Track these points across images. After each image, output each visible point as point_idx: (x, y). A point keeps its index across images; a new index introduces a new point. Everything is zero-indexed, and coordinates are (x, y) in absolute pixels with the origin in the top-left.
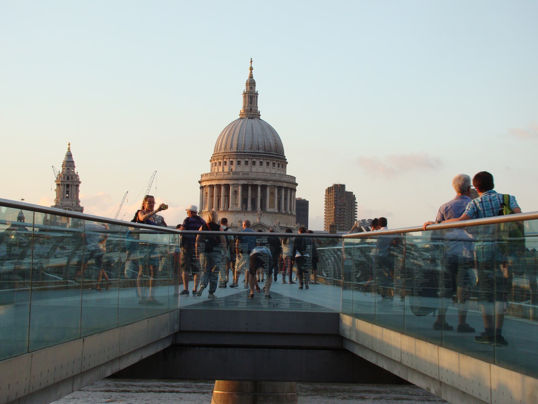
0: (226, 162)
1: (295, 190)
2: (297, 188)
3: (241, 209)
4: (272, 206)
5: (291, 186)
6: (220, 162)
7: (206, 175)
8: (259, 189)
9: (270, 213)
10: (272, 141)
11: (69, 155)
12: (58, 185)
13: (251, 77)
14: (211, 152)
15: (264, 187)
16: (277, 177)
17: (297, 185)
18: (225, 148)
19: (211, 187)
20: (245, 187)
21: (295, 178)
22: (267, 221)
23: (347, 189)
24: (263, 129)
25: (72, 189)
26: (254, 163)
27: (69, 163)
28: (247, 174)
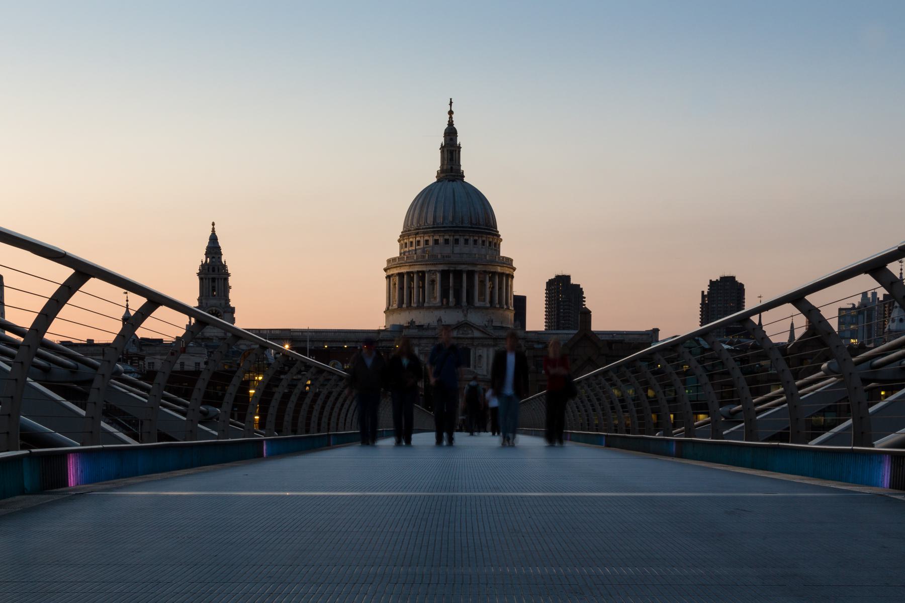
0: (419, 242)
1: (513, 277)
2: (515, 274)
3: (440, 304)
5: (507, 271)
6: (412, 242)
7: (394, 259)
8: (465, 277)
9: (479, 308)
11: (214, 239)
12: (201, 279)
14: (399, 229)
17: (514, 269)
18: (418, 222)
19: (401, 275)
20: (445, 274)
21: (512, 260)
22: (475, 318)
26: (457, 241)
27: (214, 249)
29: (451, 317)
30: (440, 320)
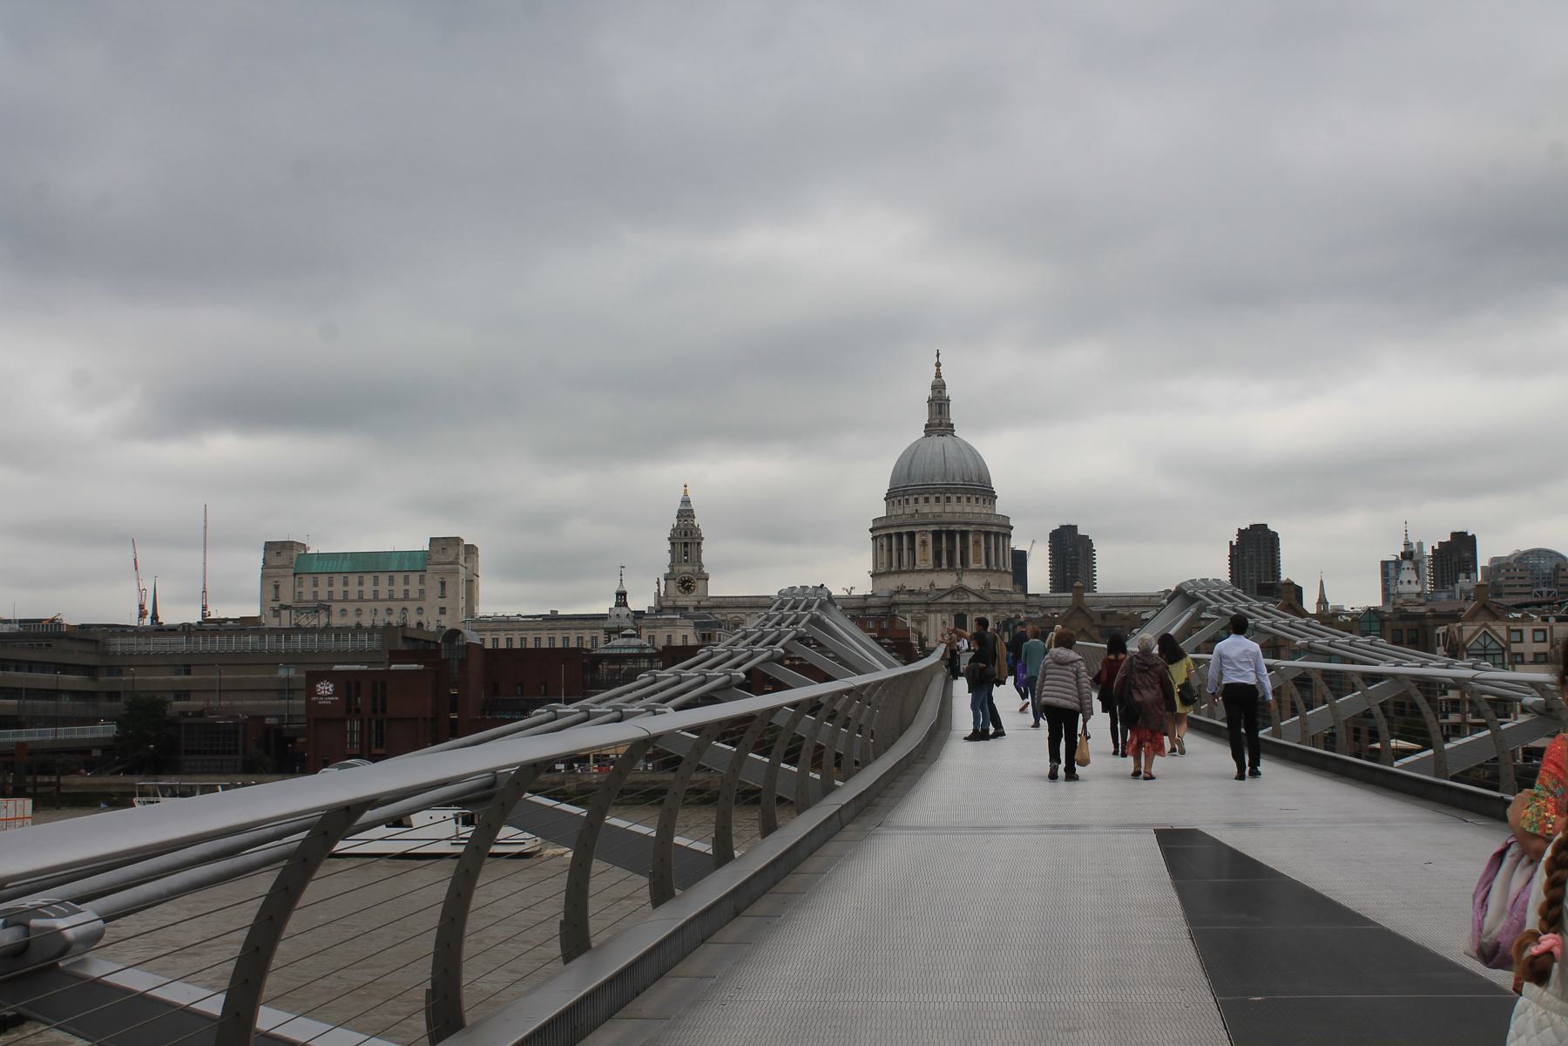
4: (977, 561)
5: (1003, 530)
10: (972, 465)
11: (686, 501)
12: (673, 544)
13: (938, 375)
15: (964, 534)
16: (983, 519)
19: (889, 536)
20: (937, 535)
22: (972, 582)
23: (1081, 532)
24: (959, 450)
25: (692, 549)
26: (948, 499)
27: (686, 513)
28: (939, 515)
29: (945, 581)
30: (932, 585)
